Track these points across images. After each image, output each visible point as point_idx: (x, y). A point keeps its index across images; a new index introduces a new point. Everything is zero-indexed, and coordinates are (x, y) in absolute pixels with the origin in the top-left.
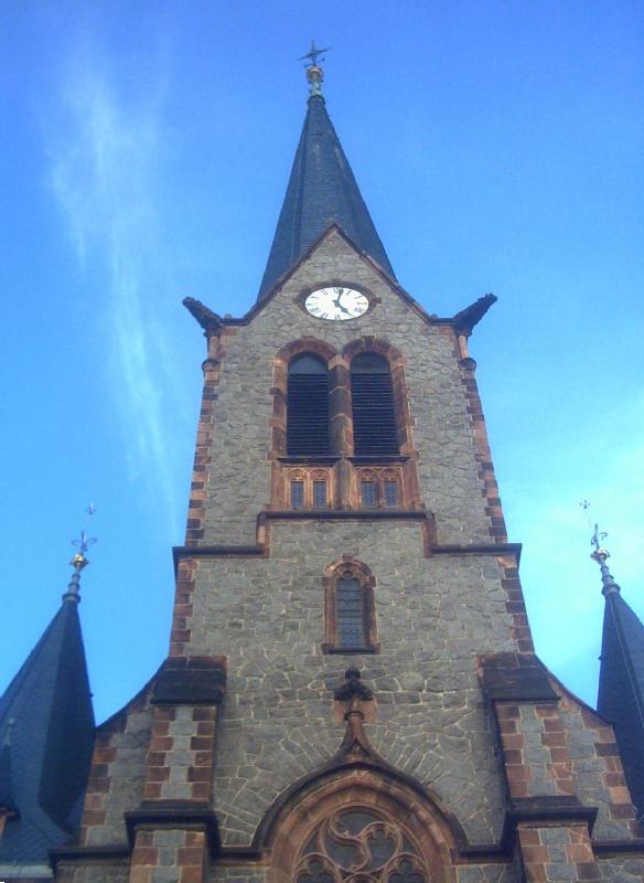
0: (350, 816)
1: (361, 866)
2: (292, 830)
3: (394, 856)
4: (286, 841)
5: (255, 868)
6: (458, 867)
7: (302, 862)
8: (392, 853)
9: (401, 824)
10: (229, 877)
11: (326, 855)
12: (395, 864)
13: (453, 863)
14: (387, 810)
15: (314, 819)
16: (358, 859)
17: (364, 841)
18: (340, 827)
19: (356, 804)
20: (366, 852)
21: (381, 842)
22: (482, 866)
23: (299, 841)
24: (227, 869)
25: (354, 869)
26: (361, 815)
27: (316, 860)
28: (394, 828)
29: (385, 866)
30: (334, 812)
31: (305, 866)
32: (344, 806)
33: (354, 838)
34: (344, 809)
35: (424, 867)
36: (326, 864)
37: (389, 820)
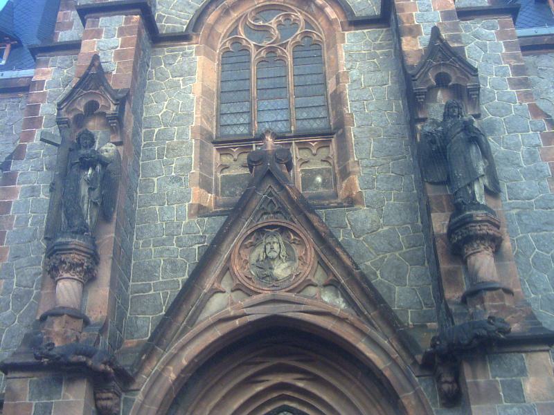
0: (265, 12)
1: (272, 41)
2: (217, 21)
3: (299, 32)
4: (212, 28)
5: (187, 47)
6: (346, 33)
7: (225, 43)
8: (297, 31)
9: (304, 12)
10: (166, 54)
11: (244, 37)
12: (298, 39)
13: (343, 30)
14: (292, 5)
15: (235, 15)
16: (270, 37)
17: (274, 26)
18: (256, 19)
19: (268, 3)
20: (276, 33)
21: (288, 26)
22: (365, 31)
23: (222, 29)
24: (165, 49)
25: (266, 43)
26: (273, 11)
27: (236, 41)
28: (299, 16)
29: (290, 40)
30: (251, 9)
31: (228, 45)
32: (259, 5)
33: (266, 24)
34: (259, 7)
35: (321, 39)
36: (244, 43)
37: (293, 11)
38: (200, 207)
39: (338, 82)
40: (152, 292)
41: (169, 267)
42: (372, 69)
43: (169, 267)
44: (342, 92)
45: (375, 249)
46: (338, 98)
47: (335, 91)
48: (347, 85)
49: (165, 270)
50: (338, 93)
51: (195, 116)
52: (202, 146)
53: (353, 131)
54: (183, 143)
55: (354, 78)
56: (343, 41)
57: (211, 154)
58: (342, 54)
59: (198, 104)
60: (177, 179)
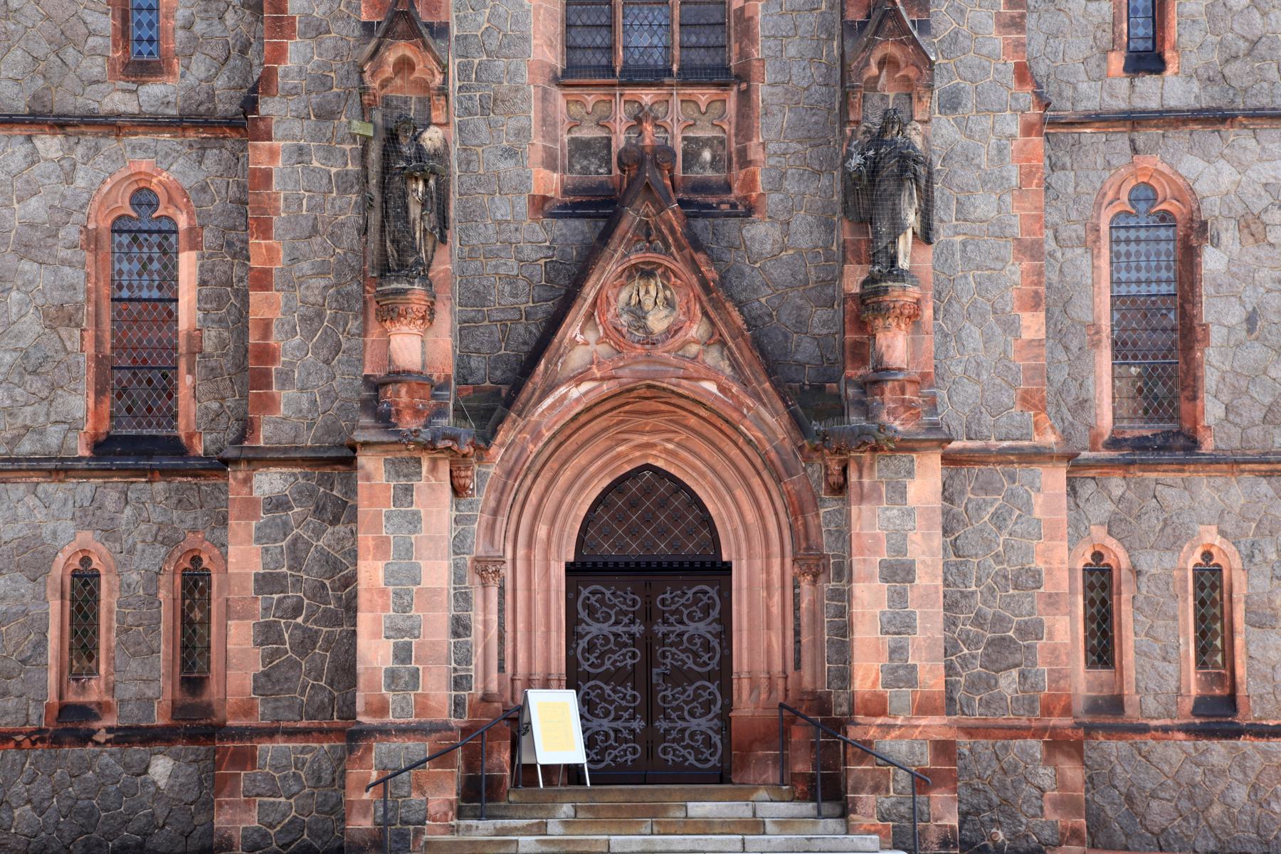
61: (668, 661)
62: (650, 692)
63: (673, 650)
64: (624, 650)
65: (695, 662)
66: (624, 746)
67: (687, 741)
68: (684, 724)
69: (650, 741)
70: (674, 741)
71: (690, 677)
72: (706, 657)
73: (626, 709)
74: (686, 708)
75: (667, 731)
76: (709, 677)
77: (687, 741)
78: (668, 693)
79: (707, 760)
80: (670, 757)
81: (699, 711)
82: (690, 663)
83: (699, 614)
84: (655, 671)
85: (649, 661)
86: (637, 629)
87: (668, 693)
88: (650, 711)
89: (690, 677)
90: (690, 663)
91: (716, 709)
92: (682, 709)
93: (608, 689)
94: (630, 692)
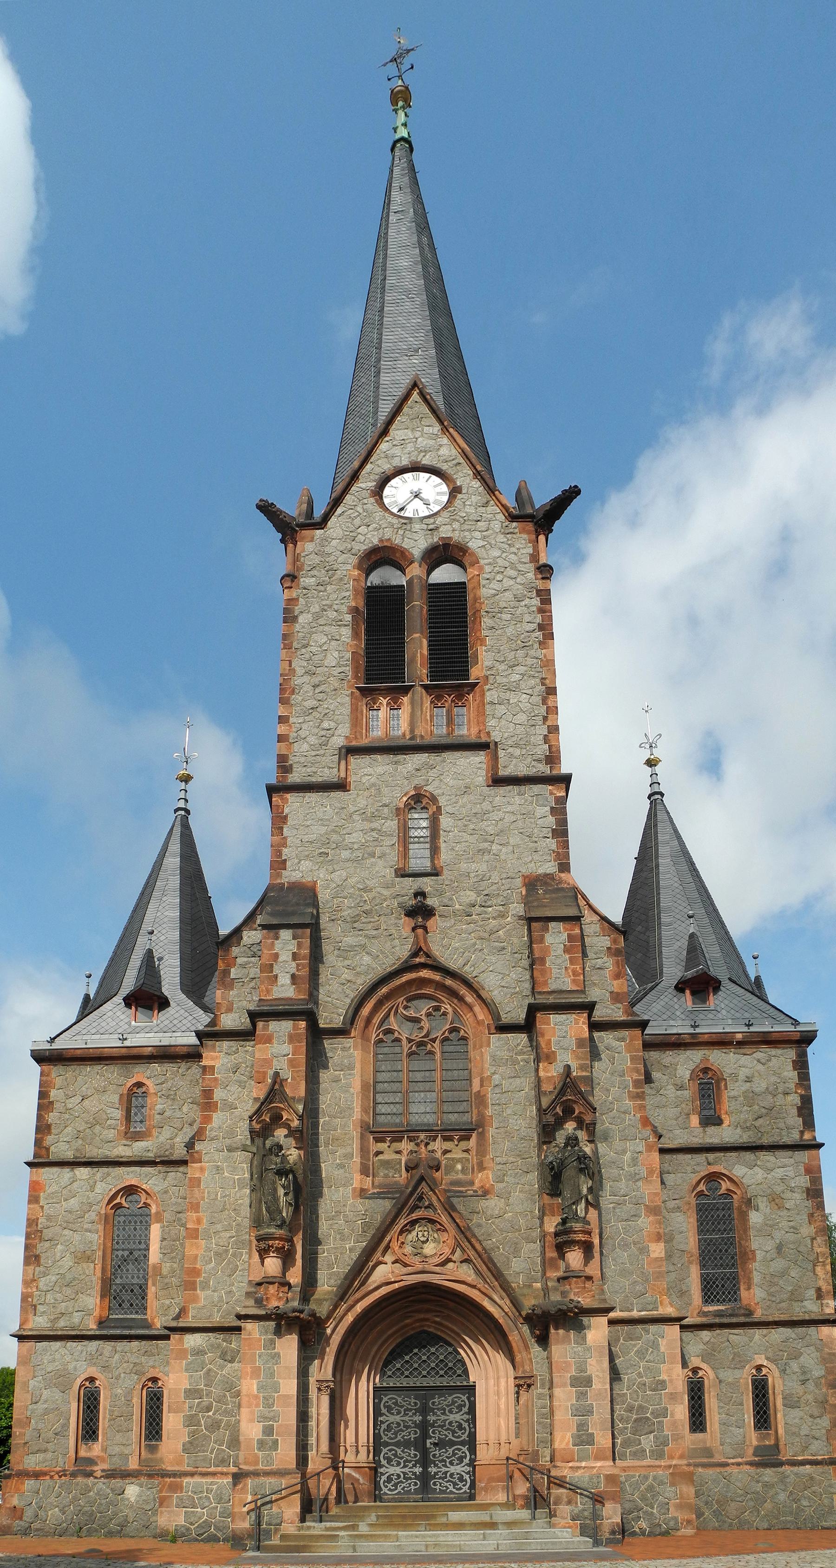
22: (509, 1035)
38: (362, 1190)
39: (482, 1085)
40: (325, 1254)
41: (338, 1237)
42: (513, 1075)
43: (338, 1237)
44: (485, 1095)
45: (501, 1230)
46: (481, 1099)
47: (479, 1092)
48: (489, 1089)
49: (335, 1239)
50: (482, 1094)
51: (356, 1110)
52: (362, 1137)
53: (491, 1132)
54: (345, 1134)
55: (497, 1083)
56: (489, 1045)
57: (369, 1142)
58: (488, 1058)
59: (358, 1098)
60: (341, 1166)
61: (437, 1435)
62: (425, 1452)
63: (440, 1429)
64: (409, 1430)
65: (453, 1436)
66: (409, 1481)
67: (448, 1478)
68: (447, 1469)
69: (425, 1479)
70: (440, 1478)
71: (452, 1443)
72: (460, 1433)
73: (410, 1461)
74: (448, 1461)
75: (436, 1473)
76: (463, 1443)
77: (448, 1478)
78: (437, 1452)
79: (461, 1489)
80: (438, 1487)
81: (456, 1462)
82: (450, 1436)
83: (455, 1410)
84: (428, 1441)
85: (425, 1436)
86: (418, 1418)
87: (437, 1452)
88: (425, 1461)
89: (452, 1443)
90: (450, 1436)
91: (467, 1461)
92: (445, 1461)
93: (399, 1451)
94: (413, 1452)
